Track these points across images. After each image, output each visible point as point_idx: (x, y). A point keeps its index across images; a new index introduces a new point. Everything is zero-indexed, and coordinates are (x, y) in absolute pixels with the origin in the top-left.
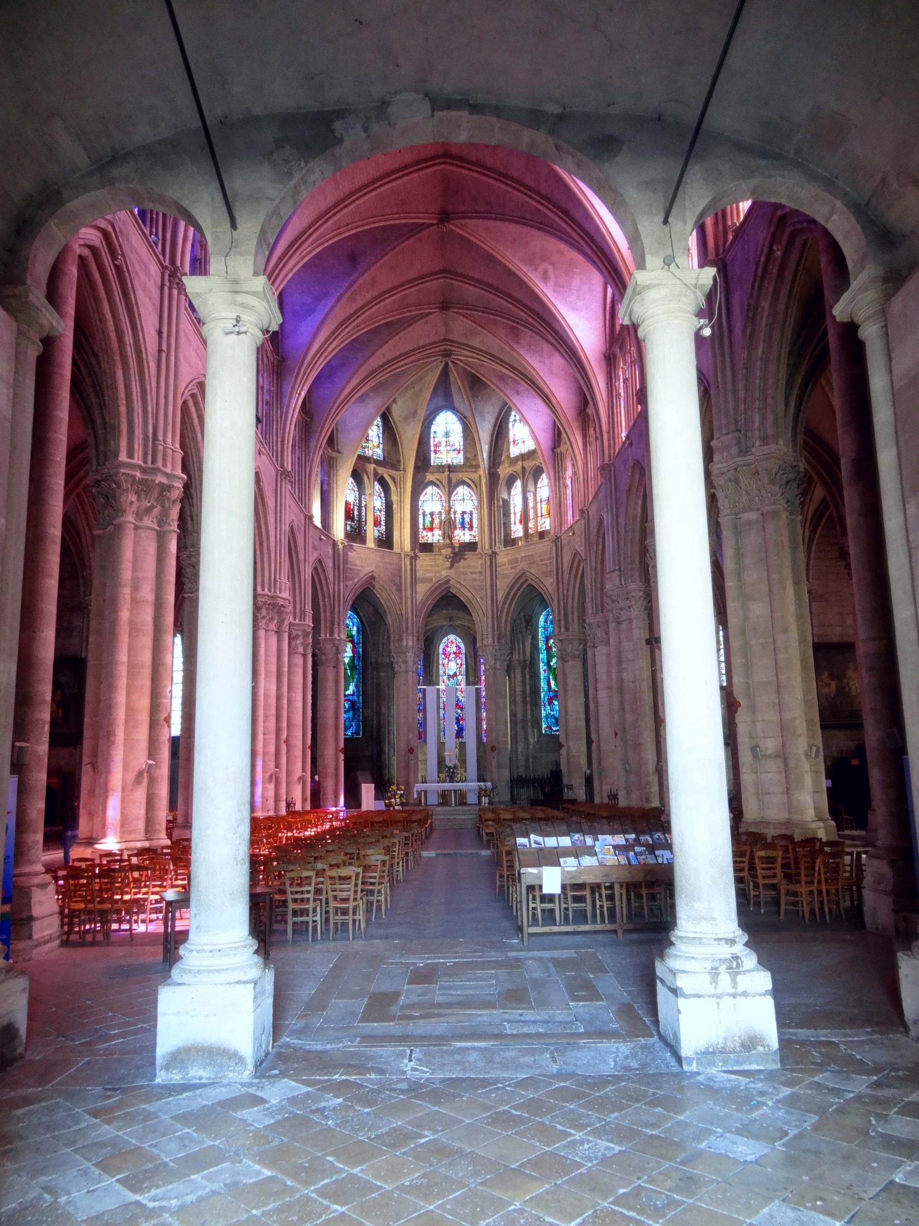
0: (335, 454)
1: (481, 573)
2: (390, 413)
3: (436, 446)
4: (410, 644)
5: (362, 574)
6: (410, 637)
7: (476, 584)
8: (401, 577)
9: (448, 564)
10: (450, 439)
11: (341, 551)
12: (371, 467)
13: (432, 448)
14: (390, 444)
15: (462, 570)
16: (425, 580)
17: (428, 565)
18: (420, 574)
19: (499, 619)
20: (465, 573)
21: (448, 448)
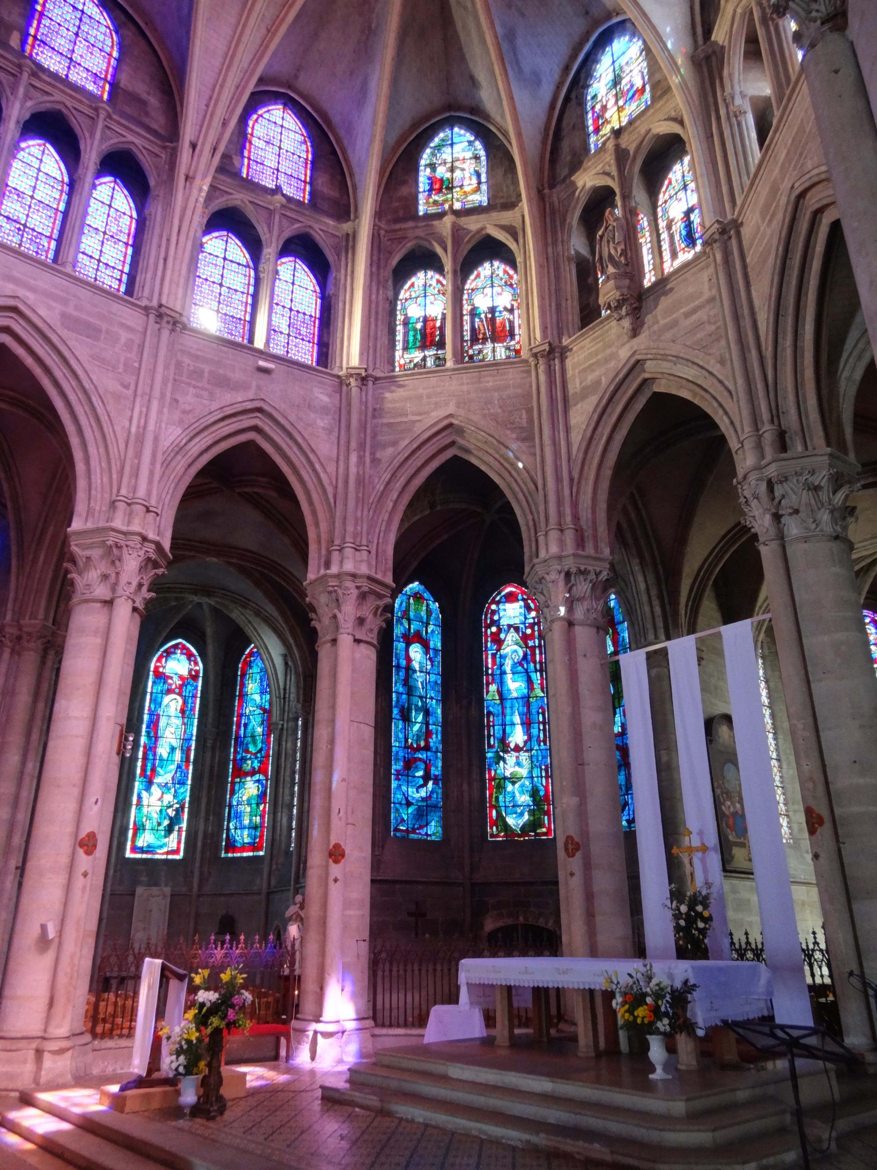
0: (346, 227)
1: (712, 300)
2: (487, 117)
3: (596, 120)
4: (554, 549)
5: (418, 429)
6: (554, 535)
7: (699, 336)
8: (530, 411)
9: (627, 323)
10: (624, 82)
11: (355, 391)
12: (448, 220)
13: (591, 129)
14: (500, 172)
15: (662, 322)
16: (585, 393)
17: (591, 355)
18: (574, 386)
19: (773, 389)
20: (675, 324)
21: (621, 103)
